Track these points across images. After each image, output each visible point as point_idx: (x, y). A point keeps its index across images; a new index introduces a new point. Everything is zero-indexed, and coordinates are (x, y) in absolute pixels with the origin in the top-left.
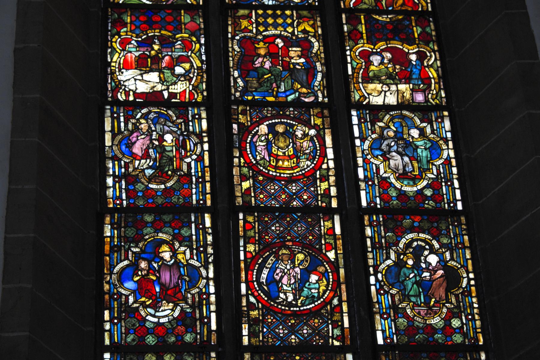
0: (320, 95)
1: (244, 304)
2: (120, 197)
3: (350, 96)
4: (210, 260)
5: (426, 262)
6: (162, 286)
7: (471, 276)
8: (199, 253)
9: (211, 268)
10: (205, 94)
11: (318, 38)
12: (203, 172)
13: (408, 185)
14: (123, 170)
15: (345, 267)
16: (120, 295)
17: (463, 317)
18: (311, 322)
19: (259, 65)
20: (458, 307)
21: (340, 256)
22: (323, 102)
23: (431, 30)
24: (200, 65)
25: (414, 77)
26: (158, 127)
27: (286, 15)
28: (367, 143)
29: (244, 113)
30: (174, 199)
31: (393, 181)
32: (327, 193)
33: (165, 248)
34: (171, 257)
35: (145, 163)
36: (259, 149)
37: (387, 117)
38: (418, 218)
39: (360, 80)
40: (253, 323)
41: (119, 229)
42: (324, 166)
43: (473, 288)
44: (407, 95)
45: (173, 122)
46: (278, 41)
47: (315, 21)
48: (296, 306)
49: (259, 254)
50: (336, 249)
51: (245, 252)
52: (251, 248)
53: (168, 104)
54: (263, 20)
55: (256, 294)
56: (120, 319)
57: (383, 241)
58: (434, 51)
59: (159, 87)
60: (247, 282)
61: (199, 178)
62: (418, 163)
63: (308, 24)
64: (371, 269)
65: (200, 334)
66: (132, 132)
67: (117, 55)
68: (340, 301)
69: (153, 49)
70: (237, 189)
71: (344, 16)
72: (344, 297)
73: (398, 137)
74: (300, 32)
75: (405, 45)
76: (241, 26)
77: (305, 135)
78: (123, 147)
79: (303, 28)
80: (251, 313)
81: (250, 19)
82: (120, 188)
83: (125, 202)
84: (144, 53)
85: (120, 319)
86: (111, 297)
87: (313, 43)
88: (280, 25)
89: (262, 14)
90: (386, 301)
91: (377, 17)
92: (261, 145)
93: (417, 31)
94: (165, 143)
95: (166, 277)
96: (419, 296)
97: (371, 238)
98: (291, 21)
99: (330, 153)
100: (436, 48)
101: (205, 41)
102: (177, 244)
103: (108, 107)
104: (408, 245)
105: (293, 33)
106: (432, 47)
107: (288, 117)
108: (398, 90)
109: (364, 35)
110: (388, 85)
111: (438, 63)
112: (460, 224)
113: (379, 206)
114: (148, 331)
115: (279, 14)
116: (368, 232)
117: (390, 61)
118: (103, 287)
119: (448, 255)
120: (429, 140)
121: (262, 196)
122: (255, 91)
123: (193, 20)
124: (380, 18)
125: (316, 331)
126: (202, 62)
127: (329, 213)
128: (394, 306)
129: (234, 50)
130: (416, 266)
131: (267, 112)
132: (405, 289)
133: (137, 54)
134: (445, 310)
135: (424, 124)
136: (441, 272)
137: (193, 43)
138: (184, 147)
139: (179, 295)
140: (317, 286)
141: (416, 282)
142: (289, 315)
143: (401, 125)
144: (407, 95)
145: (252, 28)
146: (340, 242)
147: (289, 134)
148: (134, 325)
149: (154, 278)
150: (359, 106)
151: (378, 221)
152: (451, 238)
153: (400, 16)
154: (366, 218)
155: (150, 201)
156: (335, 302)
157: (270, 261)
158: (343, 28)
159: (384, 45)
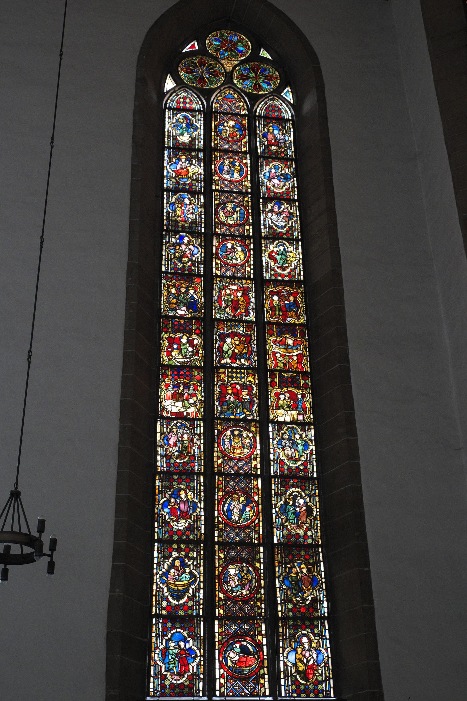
0: (255, 415)
1: (216, 521)
2: (163, 466)
3: (269, 416)
4: (202, 499)
5: (298, 503)
6: (180, 511)
7: (318, 510)
8: (197, 495)
9: (202, 502)
10: (203, 414)
12: (201, 454)
13: (293, 463)
14: (165, 452)
15: (262, 504)
16: (162, 515)
17: (313, 531)
18: (245, 531)
19: (228, 399)
20: (311, 525)
21: (260, 499)
22: (256, 419)
24: (201, 398)
25: (299, 407)
26: (181, 430)
28: (275, 441)
29: (220, 424)
30: (187, 468)
31: (286, 461)
32: (256, 467)
33: (182, 492)
34: (185, 497)
35: (175, 449)
36: (226, 443)
37: (286, 428)
38: (296, 481)
39: (274, 408)
40: (220, 530)
41: (162, 482)
42: (255, 453)
43: (318, 516)
44: (295, 417)
45: (188, 428)
47: (255, 376)
48: (239, 523)
49: (224, 497)
50: (258, 495)
51: (218, 495)
52: (220, 493)
53: (185, 419)
55: (222, 516)
56: (162, 527)
57: (280, 492)
58: (309, 393)
59: (182, 410)
60: (218, 510)
61: (199, 457)
62: (298, 452)
64: (273, 506)
65: (196, 535)
66: (169, 433)
67: (163, 392)
68: (259, 521)
69: (180, 389)
70: (216, 463)
71: (269, 373)
72: (261, 519)
73: (290, 439)
77: (248, 436)
78: (165, 441)
80: (219, 525)
82: (163, 461)
83: (165, 469)
84: (175, 392)
85: (162, 527)
86: (158, 516)
90: (279, 522)
91: (284, 374)
92: (227, 441)
93: (302, 382)
94: (184, 439)
95: (182, 506)
96: (294, 519)
97: (274, 490)
99: (258, 446)
100: (310, 392)
102: (188, 491)
103: (159, 420)
104: (291, 494)
105: (244, 382)
107: (240, 427)
108: (291, 414)
110: (287, 411)
111: (311, 399)
112: (315, 484)
113: (279, 474)
114: (174, 533)
116: (273, 487)
117: (289, 398)
118: (155, 511)
119: (308, 500)
120: (304, 441)
121: (226, 467)
122: (226, 413)
123: (199, 374)
124: (285, 375)
125: (247, 535)
126: (202, 396)
127: (256, 477)
128: (282, 525)
129: (217, 390)
130: (294, 505)
131: (231, 424)
132: (288, 516)
133: (173, 392)
134: (305, 527)
135: (302, 432)
136: (304, 508)
138: (192, 441)
139: (188, 516)
140: (249, 513)
141: (293, 513)
142: (236, 527)
143: (292, 433)
144: (295, 417)
146: (260, 492)
147: (240, 436)
148: (168, 530)
149: (177, 507)
150: (273, 422)
151: (278, 482)
152: (310, 491)
154: (273, 480)
155: (177, 468)
156: (257, 521)
157: (228, 500)
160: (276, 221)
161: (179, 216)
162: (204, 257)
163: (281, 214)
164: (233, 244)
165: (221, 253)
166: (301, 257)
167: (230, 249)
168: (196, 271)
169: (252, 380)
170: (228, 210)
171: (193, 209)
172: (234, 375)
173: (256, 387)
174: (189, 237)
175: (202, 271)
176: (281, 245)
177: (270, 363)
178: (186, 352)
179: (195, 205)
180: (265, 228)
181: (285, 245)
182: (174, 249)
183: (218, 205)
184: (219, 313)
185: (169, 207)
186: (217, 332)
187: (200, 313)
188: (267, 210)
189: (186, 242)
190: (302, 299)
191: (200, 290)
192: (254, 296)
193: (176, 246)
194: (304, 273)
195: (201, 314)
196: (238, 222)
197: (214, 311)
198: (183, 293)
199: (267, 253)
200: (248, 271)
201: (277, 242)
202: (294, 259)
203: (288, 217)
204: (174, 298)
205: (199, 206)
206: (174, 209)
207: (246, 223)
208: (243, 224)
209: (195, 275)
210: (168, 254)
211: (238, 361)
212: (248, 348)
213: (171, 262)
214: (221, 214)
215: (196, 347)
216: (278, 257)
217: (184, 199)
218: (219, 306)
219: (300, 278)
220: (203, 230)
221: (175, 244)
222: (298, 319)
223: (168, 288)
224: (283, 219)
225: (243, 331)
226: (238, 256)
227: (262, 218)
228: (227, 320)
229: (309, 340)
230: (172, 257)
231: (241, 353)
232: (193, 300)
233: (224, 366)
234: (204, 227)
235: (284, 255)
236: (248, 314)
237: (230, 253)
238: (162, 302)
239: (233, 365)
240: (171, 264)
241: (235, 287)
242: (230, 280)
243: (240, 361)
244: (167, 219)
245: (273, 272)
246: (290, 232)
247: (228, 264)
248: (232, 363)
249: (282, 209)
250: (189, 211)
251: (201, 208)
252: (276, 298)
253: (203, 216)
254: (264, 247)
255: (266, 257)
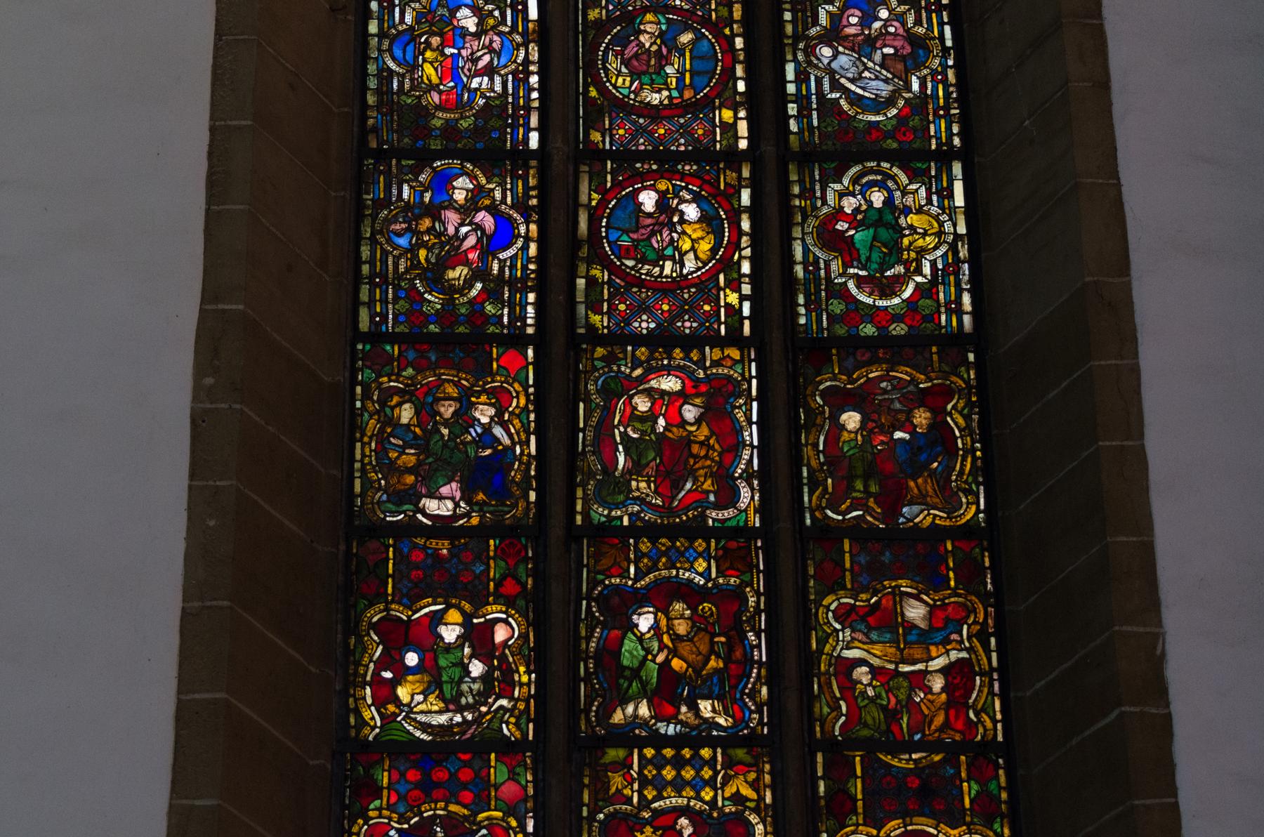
11: (763, 814)
23: (1000, 788)
27: (701, 758)
46: (683, 821)
47: (760, 772)
54: (654, 772)
63: (746, 782)
74: (728, 799)
75: (942, 825)
76: (609, 789)
79: (734, 790)
81: (629, 772)
87: (753, 826)
88: (688, 783)
89: (654, 757)
91: (888, 759)
93: (969, 790)
98: (710, 773)
101: (534, 827)
106: (999, 830)
109: (860, 804)
115: (688, 756)
123: (513, 776)
124: (895, 762)
137: (511, 832)
145: (630, 793)
153: (937, 754)
158: (816, 787)
159: (899, 828)
160: (852, 81)
161: (432, 87)
162: (541, 258)
163: (875, 49)
164: (663, 196)
165: (612, 238)
166: (962, 229)
167: (650, 215)
168: (506, 320)
169: (747, 791)
170: (641, 45)
171: (491, 50)
172: (669, 773)
173: (764, 821)
174: (473, 177)
175: (530, 321)
176: (872, 184)
177: (826, 710)
178: (461, 681)
179: (500, 34)
180: (803, 113)
181: (890, 184)
182: (408, 229)
183: (601, 27)
184: (604, 504)
185: (390, 50)
186: (593, 583)
187: (522, 505)
188: (813, 31)
189: (460, 196)
190: (967, 418)
191: (523, 402)
192: (755, 418)
193: (418, 218)
194: (973, 303)
195: (528, 509)
196: (688, 94)
197: (579, 493)
198: (446, 423)
199: (812, 222)
200: (728, 305)
201: (854, 170)
202: (930, 241)
203: (904, 59)
204: (407, 445)
205: (518, 39)
206: (409, 56)
207: (719, 96)
208: (707, 105)
209: (501, 340)
210: (385, 253)
211: (684, 709)
212: (730, 646)
213: (397, 288)
214: (614, 64)
215: (503, 658)
216: (861, 237)
217: (453, 12)
218: (605, 471)
219: (960, 322)
220: (534, 140)
221: (413, 212)
222: (951, 507)
223: (383, 402)
224: (882, 66)
225: (706, 574)
226: (686, 245)
227: (790, 71)
228: (637, 530)
229: (997, 599)
230: (402, 268)
231: (698, 672)
232: (488, 452)
233: (628, 737)
234: (541, 129)
235: (887, 226)
236: (728, 497)
237: (653, 233)
238: (357, 465)
239: (662, 728)
240: (396, 299)
241: (670, 384)
242: (652, 353)
243: (694, 708)
244: (378, 107)
245: (837, 307)
246: (915, 122)
247: (641, 283)
248: (658, 717)
249: (877, 25)
250: (475, 61)
251: (525, 45)
252: (851, 419)
253: (534, 80)
254: (800, 196)
255: (809, 240)
